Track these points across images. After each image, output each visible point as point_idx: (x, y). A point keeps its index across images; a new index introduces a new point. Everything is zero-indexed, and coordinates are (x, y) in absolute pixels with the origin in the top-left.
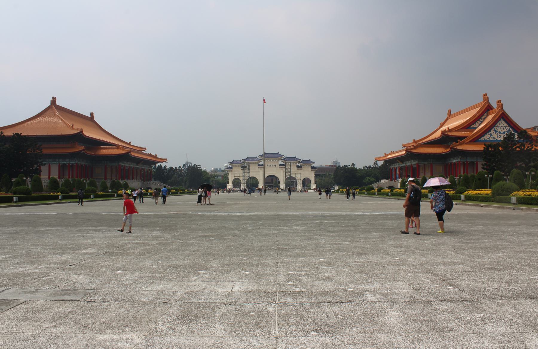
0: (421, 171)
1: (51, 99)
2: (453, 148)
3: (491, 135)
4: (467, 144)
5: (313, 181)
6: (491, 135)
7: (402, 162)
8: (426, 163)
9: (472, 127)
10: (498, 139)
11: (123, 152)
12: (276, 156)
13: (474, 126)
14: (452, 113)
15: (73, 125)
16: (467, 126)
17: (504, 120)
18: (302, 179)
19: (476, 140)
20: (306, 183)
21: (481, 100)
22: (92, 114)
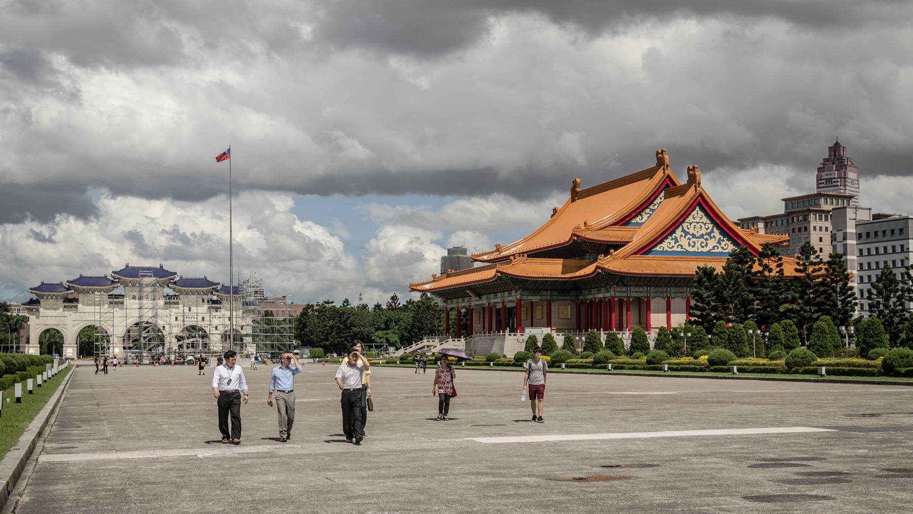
3: (676, 241)
4: (625, 257)
6: (676, 241)
7: (479, 295)
8: (535, 298)
9: (634, 221)
10: (691, 249)
16: (624, 221)
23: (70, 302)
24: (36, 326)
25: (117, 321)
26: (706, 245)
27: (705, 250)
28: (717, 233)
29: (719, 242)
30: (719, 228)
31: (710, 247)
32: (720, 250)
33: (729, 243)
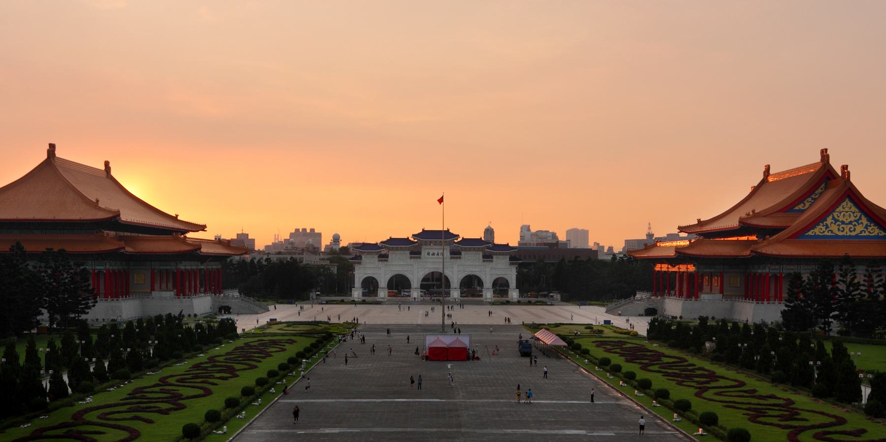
0: (705, 283)
2: (756, 252)
3: (827, 227)
5: (513, 283)
6: (827, 227)
9: (797, 208)
10: (840, 234)
12: (442, 237)
13: (801, 206)
14: (771, 172)
15: (98, 201)
16: (788, 208)
17: (852, 200)
18: (495, 277)
19: (799, 235)
20: (500, 286)
21: (817, 159)
22: (107, 164)
23: (383, 257)
24: (360, 274)
26: (854, 230)
27: (853, 234)
28: (864, 221)
29: (866, 227)
30: (866, 215)
31: (858, 231)
32: (867, 234)
33: (876, 228)
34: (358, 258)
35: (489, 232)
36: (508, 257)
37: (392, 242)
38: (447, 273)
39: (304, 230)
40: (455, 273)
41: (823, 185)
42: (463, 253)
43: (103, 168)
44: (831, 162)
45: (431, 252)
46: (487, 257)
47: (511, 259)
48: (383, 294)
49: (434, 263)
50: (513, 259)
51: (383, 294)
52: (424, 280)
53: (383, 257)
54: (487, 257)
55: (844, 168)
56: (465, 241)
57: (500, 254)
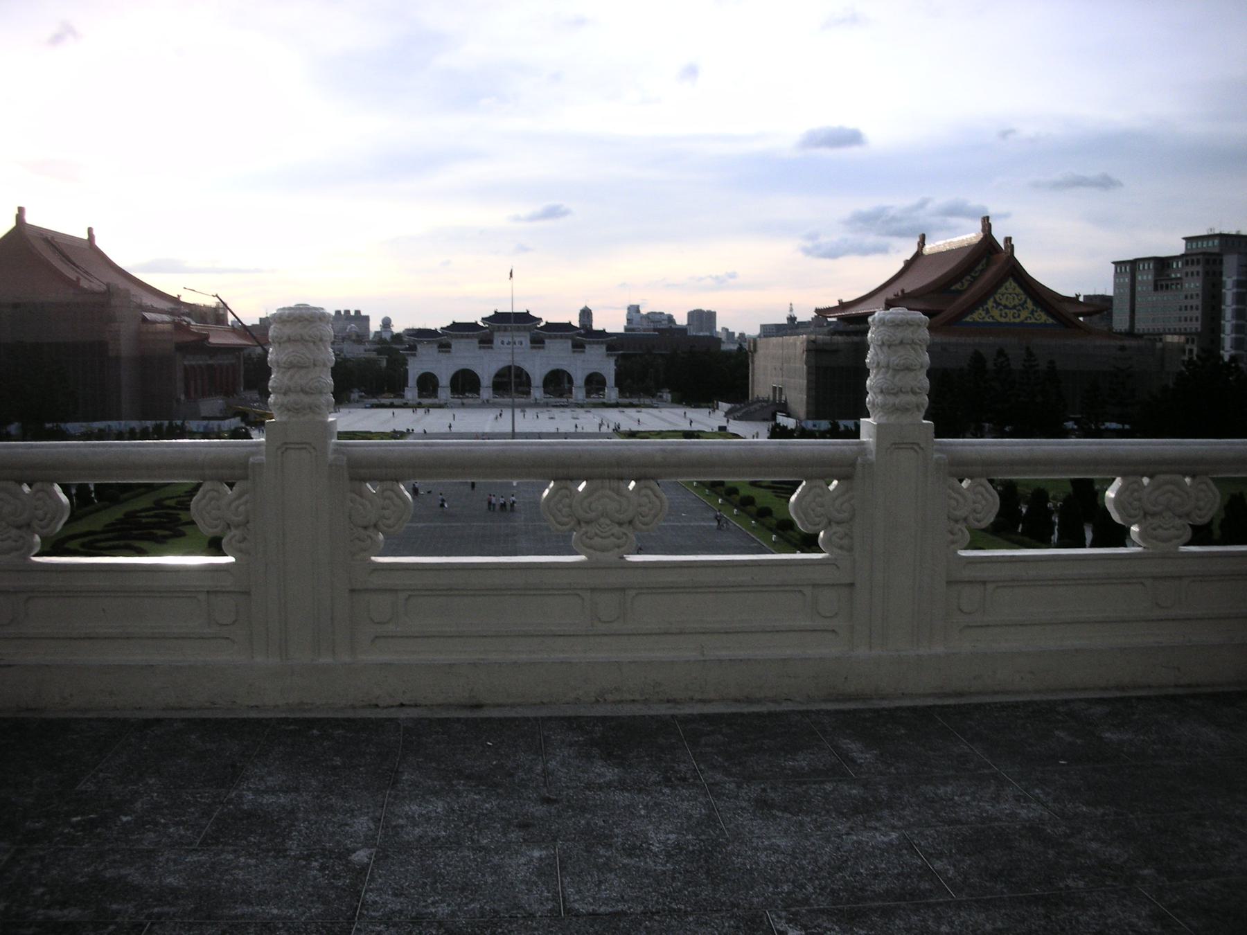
1: (16, 212)
3: (987, 311)
6: (987, 311)
10: (1003, 320)
11: (193, 338)
12: (524, 319)
13: (957, 286)
17: (1016, 280)
18: (587, 372)
22: (90, 230)
23: (445, 347)
24: (415, 369)
25: (487, 366)
27: (1017, 320)
28: (1030, 304)
29: (1032, 312)
30: (1033, 299)
31: (1022, 317)
33: (1042, 314)
34: (413, 348)
35: (586, 314)
36: (604, 347)
37: (456, 327)
38: (527, 367)
39: (347, 312)
40: (537, 366)
41: (984, 261)
42: (547, 341)
43: (86, 237)
44: (994, 233)
45: (506, 340)
46: (578, 346)
47: (608, 349)
48: (444, 394)
49: (508, 355)
50: (610, 348)
51: (444, 394)
52: (498, 375)
53: (445, 347)
54: (578, 346)
55: (1008, 240)
56: (550, 326)
57: (594, 343)
